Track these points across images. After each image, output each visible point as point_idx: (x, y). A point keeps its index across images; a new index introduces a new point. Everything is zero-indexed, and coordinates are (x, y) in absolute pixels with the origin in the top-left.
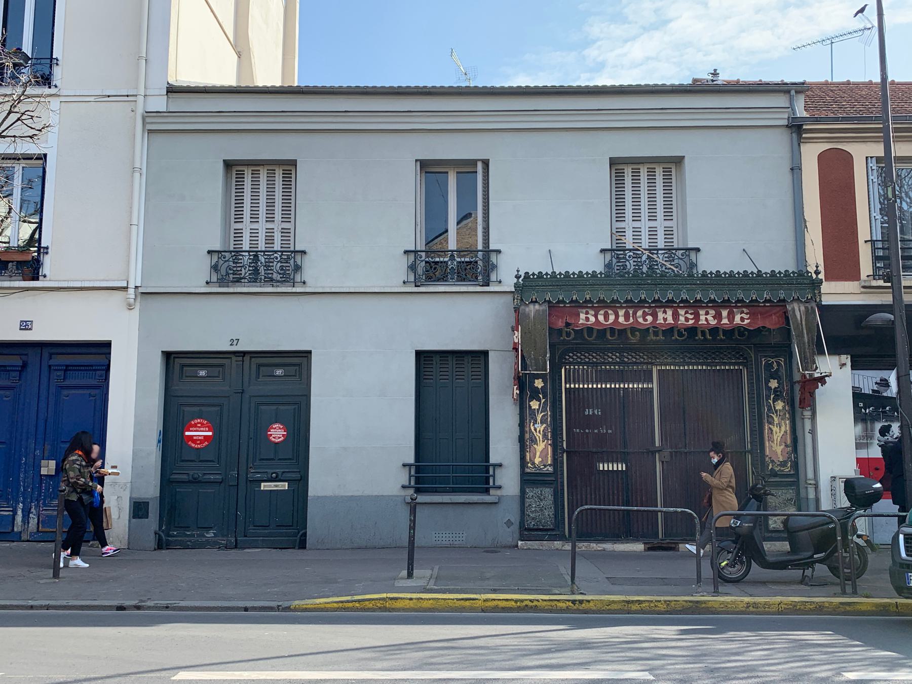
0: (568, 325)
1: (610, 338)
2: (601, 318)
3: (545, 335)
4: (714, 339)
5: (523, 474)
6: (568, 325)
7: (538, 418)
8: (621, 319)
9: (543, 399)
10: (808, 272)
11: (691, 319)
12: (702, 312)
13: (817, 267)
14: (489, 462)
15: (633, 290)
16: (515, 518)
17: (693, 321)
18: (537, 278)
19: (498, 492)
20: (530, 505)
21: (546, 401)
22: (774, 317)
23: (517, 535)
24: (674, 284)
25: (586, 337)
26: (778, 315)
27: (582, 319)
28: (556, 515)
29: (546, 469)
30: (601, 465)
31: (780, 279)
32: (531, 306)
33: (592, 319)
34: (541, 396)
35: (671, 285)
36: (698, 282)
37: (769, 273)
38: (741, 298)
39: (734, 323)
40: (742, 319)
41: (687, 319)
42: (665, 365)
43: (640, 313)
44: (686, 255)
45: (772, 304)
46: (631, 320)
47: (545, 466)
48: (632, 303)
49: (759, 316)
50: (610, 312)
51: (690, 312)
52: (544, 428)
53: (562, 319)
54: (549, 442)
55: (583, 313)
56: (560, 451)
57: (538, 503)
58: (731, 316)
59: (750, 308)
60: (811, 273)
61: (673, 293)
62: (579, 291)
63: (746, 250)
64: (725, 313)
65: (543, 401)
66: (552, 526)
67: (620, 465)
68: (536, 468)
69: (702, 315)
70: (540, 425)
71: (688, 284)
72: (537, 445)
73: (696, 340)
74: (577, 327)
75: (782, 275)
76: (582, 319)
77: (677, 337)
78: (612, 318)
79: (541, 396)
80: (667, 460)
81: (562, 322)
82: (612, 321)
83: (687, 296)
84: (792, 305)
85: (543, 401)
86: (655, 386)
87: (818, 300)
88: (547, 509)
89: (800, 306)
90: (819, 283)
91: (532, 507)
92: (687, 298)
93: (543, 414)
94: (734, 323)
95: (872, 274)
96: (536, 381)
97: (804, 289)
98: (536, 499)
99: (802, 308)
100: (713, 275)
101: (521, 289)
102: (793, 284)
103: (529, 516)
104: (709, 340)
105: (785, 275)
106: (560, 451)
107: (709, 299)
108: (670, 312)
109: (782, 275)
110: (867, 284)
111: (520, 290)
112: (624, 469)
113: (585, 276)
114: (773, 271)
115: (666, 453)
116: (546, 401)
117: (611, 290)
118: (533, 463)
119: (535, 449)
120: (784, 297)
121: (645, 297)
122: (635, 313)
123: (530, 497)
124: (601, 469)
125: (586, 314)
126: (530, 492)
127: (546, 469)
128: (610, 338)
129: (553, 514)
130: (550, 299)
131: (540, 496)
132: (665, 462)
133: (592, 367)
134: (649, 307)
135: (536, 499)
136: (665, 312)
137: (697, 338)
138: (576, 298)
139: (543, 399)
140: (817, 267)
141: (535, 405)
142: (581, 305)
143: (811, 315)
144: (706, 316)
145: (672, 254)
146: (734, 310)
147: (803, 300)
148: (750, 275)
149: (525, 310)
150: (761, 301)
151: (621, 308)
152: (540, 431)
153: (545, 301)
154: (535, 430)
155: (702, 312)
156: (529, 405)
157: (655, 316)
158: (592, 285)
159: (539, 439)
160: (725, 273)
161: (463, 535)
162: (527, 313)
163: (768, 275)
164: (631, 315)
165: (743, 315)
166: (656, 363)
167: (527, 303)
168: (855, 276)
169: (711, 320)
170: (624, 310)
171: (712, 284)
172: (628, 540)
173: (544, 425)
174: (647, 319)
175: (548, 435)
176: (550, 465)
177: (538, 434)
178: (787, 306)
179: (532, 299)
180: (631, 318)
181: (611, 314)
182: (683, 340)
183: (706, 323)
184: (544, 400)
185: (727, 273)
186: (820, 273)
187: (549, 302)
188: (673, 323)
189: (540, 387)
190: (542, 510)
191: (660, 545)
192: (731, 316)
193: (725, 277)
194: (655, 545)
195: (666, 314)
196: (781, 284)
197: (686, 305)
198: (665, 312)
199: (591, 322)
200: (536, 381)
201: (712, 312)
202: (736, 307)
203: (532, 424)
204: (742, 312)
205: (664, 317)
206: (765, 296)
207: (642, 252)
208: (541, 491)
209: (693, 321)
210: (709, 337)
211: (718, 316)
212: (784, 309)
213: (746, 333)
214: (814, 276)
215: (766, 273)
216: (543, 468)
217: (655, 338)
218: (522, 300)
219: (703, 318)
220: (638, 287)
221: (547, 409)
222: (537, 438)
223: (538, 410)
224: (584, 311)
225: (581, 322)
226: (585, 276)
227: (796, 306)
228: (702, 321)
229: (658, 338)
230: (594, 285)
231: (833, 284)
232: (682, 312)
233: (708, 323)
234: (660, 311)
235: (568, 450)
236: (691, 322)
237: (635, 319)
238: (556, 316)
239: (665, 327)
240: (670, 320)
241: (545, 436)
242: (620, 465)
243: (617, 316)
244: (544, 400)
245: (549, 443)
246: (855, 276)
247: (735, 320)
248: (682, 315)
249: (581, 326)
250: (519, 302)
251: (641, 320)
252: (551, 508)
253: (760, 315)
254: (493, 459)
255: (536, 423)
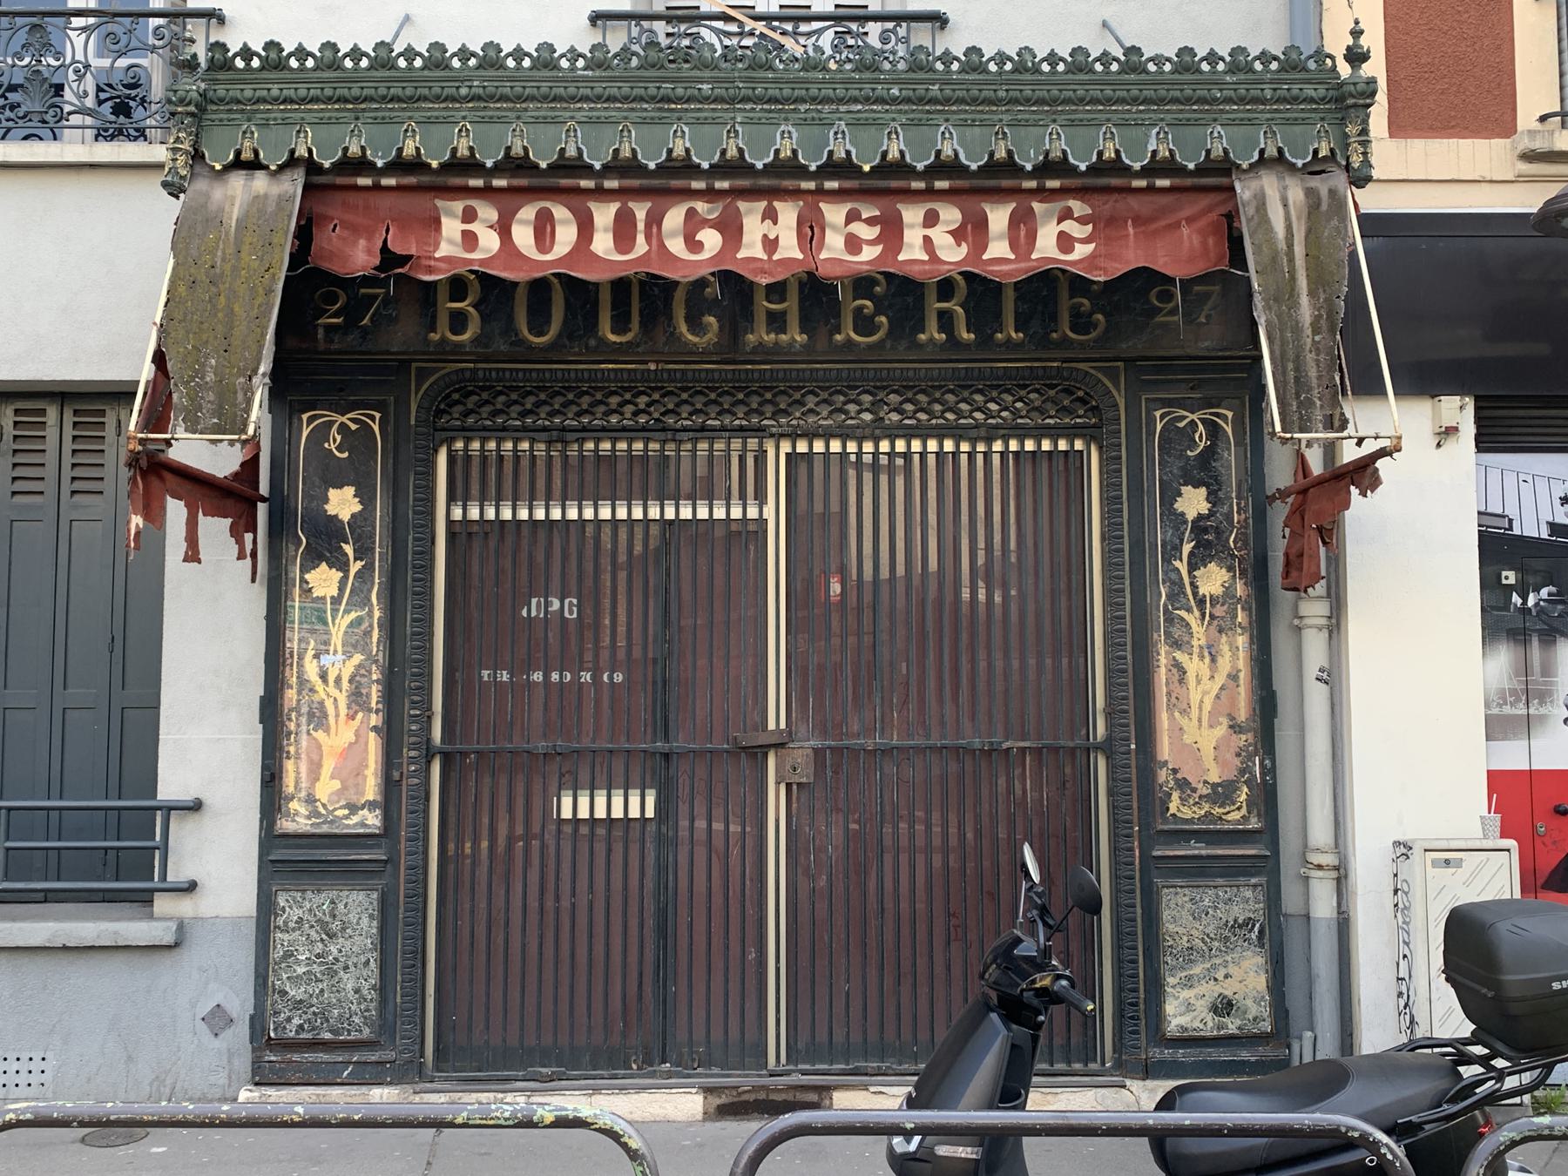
0: (390, 259)
1: (613, 338)
2: (523, 236)
3: (269, 292)
4: (985, 340)
5: (270, 838)
6: (390, 259)
7: (333, 630)
8: (602, 243)
9: (356, 559)
10: (1320, 55)
11: (872, 243)
12: (912, 215)
13: (1356, 33)
14: (154, 795)
15: (644, 122)
16: (240, 1004)
17: (877, 250)
18: (262, 68)
19: (184, 907)
20: (288, 955)
21: (369, 567)
22: (1185, 231)
23: (244, 1062)
24: (803, 101)
25: (526, 332)
26: (1202, 223)
27: (451, 242)
28: (383, 989)
29: (355, 819)
30: (567, 802)
31: (1214, 81)
32: (237, 181)
33: (490, 242)
34: (349, 549)
35: (787, 100)
36: (895, 91)
37: (1168, 60)
38: (1056, 154)
39: (1034, 256)
40: (1065, 242)
41: (853, 244)
42: (810, 436)
43: (674, 218)
44: (898, 40)
45: (1178, 181)
46: (641, 246)
47: (353, 808)
48: (645, 178)
49: (1131, 230)
50: (560, 212)
51: (863, 217)
52: (359, 666)
53: (370, 239)
54: (375, 720)
55: (451, 214)
56: (412, 754)
57: (319, 948)
58: (1023, 227)
59: (1099, 199)
60: (1332, 58)
61: (795, 135)
62: (428, 122)
63: (1113, 24)
64: (999, 217)
65: (355, 567)
66: (366, 1031)
67: (634, 801)
68: (318, 815)
69: (912, 226)
70: (340, 656)
71: (856, 100)
72: (327, 731)
73: (920, 346)
74: (430, 270)
75: (1221, 67)
76: (451, 242)
77: (853, 335)
78: (566, 235)
79: (349, 549)
80: (804, 780)
81: (369, 252)
82: (567, 250)
83: (848, 147)
84: (1254, 184)
85: (355, 567)
86: (774, 512)
87: (1356, 161)
88: (352, 969)
89: (1285, 188)
90: (1362, 94)
91: (298, 962)
92: (848, 153)
93: (353, 615)
94: (1034, 256)
95: (1558, 109)
96: (333, 494)
97: (1304, 122)
98: (313, 933)
99: (1296, 194)
100: (955, 66)
101: (192, 108)
102: (1264, 101)
103: (283, 993)
104: (967, 346)
105: (1233, 68)
106: (412, 754)
107: (932, 158)
108: (788, 213)
109: (1221, 67)
110: (1540, 145)
111: (192, 114)
112: (650, 813)
113: (456, 63)
114: (1186, 51)
115: (801, 755)
116: (369, 567)
117: (555, 121)
118: (311, 800)
119: (319, 747)
120: (1225, 150)
121: (687, 150)
122: (655, 220)
123: (292, 925)
124: (567, 813)
125: (462, 222)
126: (293, 906)
127: (355, 819)
128: (613, 338)
129: (373, 987)
130: (310, 151)
131: (328, 919)
132: (795, 787)
133: (549, 443)
134: (710, 194)
135: (313, 933)
136: (771, 215)
137: (922, 337)
138: (418, 149)
139: (356, 559)
140: (1356, 33)
141: (324, 581)
142: (440, 180)
143: (1328, 221)
144: (929, 232)
145: (848, 37)
146: (1036, 205)
147: (1300, 163)
148: (1098, 67)
149: (207, 196)
150: (1137, 166)
151: (601, 193)
152: (338, 680)
153: (292, 162)
154: (324, 676)
155: (912, 215)
156: (304, 581)
157: (731, 230)
158: (479, 98)
159: (336, 707)
160: (1001, 58)
161: (43, 1065)
162: (213, 207)
163: (1168, 67)
164: (641, 226)
165: (1069, 226)
166: (774, 430)
167: (218, 167)
168: (1504, 125)
169: (949, 247)
170: (613, 208)
171: (947, 101)
172: (652, 1075)
173: (358, 658)
174: (700, 244)
175: (368, 695)
176: (371, 805)
177: (332, 689)
178: (1238, 187)
179: (238, 153)
180: (641, 238)
181: (565, 222)
182: (870, 347)
183: (926, 258)
184: (359, 564)
185: (1010, 59)
186: (1365, 57)
187: (312, 167)
188: (801, 256)
189: (345, 516)
190: (332, 973)
191: (762, 1096)
192: (1023, 227)
193: (1001, 72)
194: (745, 1097)
195: (775, 223)
196: (1215, 101)
197: (848, 184)
198: (771, 215)
199: (487, 251)
200: (333, 494)
201: (951, 215)
202: (1042, 193)
203: (310, 653)
204: (1066, 215)
205: (765, 236)
206: (1151, 148)
207: (741, 24)
208: (332, 902)
209: (877, 250)
210: (965, 335)
211: (973, 230)
212: (1224, 202)
213: (1100, 317)
214: (1344, 70)
215: (1158, 60)
216: (346, 817)
217: (773, 336)
218: (197, 156)
219: (913, 237)
220: (660, 109)
221: (369, 600)
222: (329, 705)
223: (336, 601)
224: (458, 206)
225: (444, 250)
226: (456, 63)
227: (1269, 183)
228: (912, 250)
229: (783, 337)
230: (491, 98)
231: (1418, 146)
232: (834, 213)
233: (934, 258)
234: (750, 211)
235: (448, 748)
236: (869, 253)
237: (654, 241)
238: (346, 225)
239: (771, 274)
240: (790, 248)
241: (357, 698)
242: (634, 801)
243: (586, 227)
244: (359, 564)
245: (373, 723)
246: (1504, 125)
247: (1040, 242)
248: (834, 228)
249: (442, 265)
250: (179, 163)
251: (676, 246)
252: (367, 963)
253: (1134, 227)
254: (171, 785)
255: (327, 652)
